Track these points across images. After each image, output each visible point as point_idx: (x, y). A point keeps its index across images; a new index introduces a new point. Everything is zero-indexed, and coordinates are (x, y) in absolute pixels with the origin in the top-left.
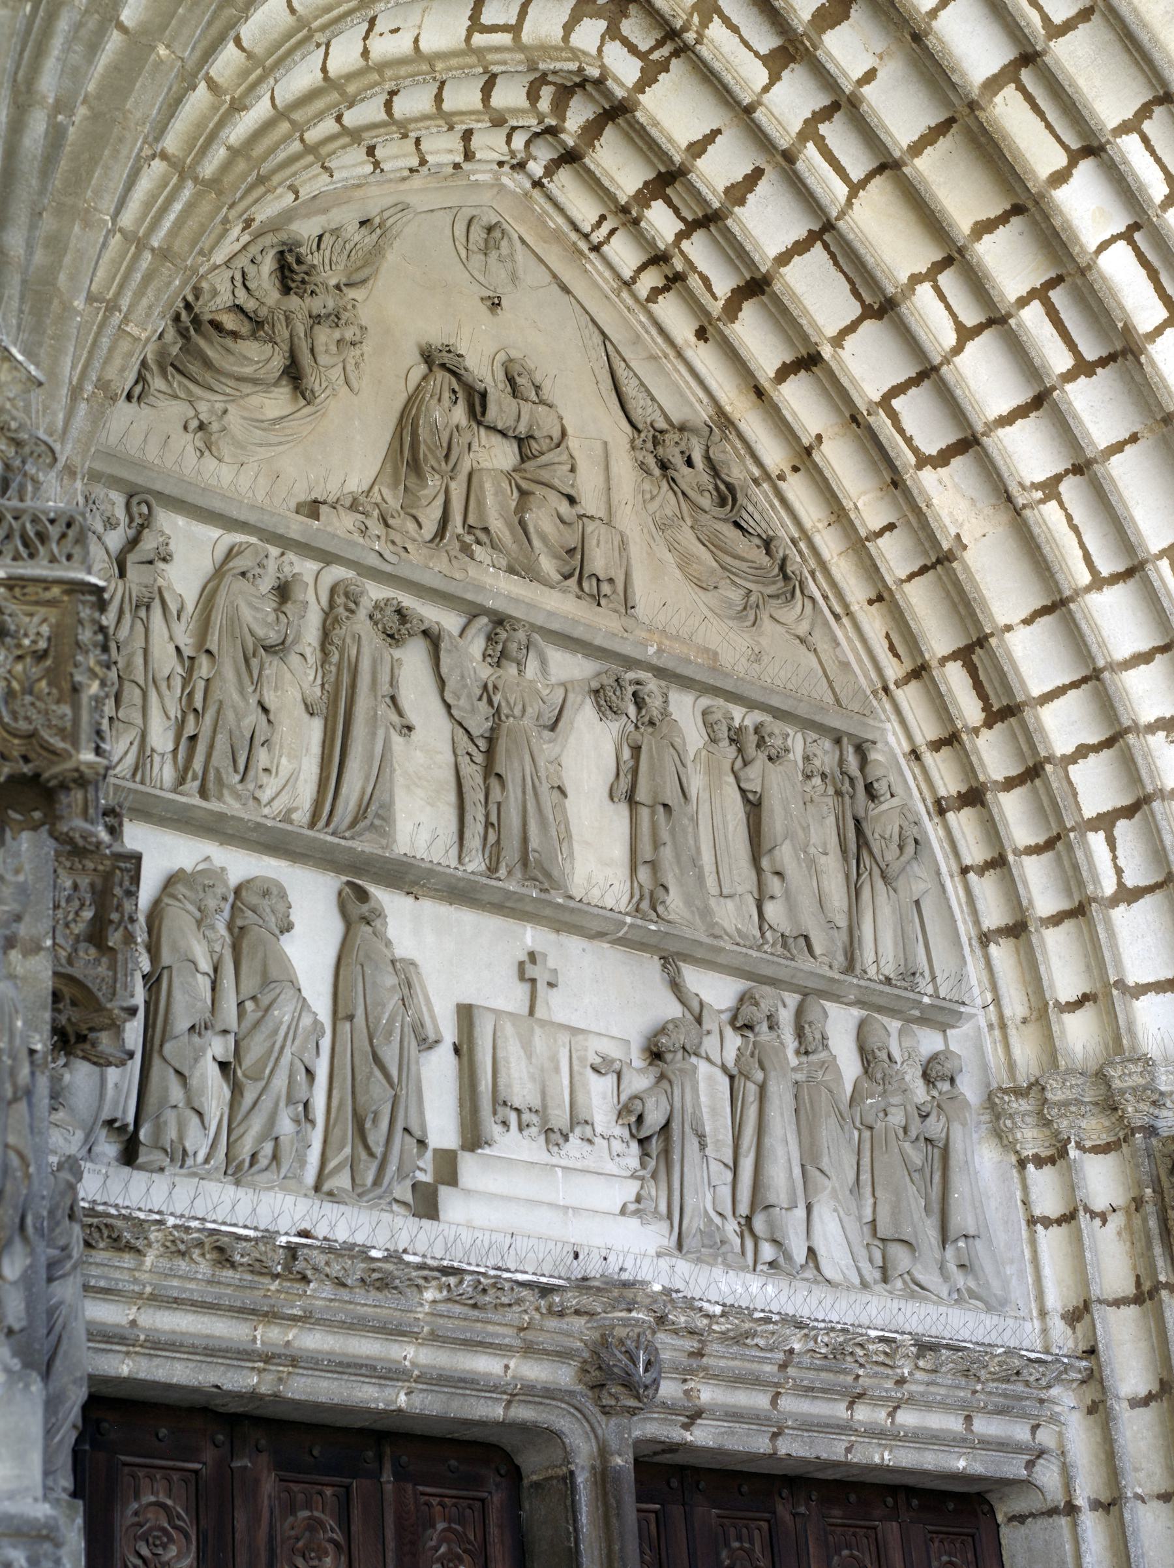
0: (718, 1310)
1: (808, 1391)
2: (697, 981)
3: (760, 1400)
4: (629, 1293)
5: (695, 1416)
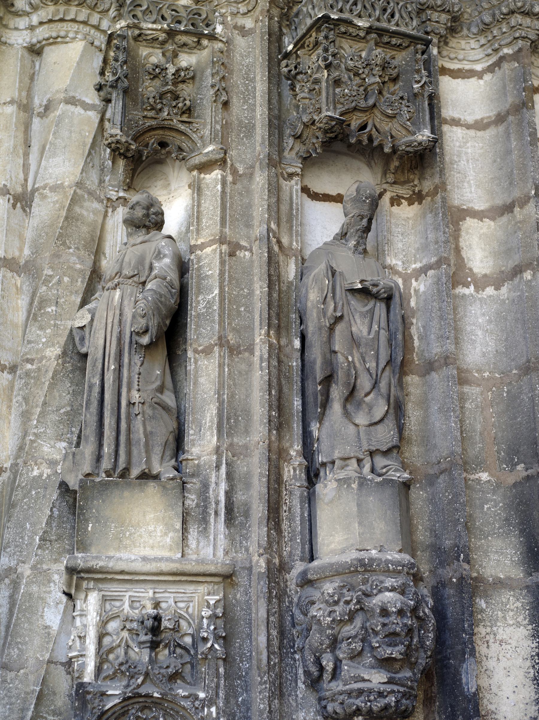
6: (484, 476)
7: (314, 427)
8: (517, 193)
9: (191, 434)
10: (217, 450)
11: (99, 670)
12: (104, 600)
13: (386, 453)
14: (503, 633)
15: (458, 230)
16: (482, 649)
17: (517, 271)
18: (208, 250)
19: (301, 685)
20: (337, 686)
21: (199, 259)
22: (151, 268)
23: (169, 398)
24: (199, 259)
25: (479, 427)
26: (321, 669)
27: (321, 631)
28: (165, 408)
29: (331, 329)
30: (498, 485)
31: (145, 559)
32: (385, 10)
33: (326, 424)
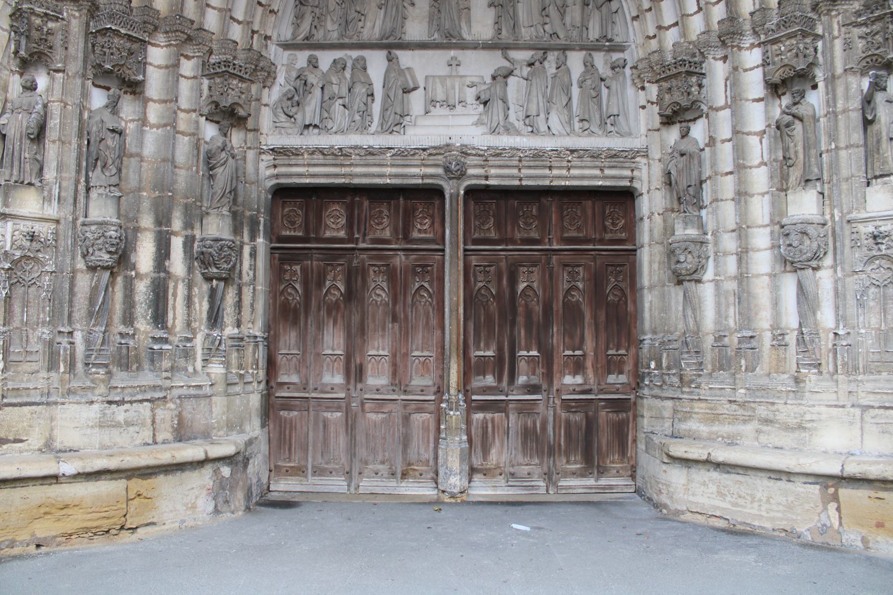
0: (486, 148)
1: (530, 167)
2: (513, 54)
3: (515, 171)
4: (449, 148)
5: (487, 178)
6: (145, 194)
7: (90, 174)
8: (169, 98)
9: (46, 170)
10: (56, 178)
11: (11, 247)
12: (14, 224)
13: (114, 186)
14: (145, 244)
15: (146, 106)
16: (138, 249)
17: (165, 125)
18: (56, 104)
19: (79, 256)
20: (93, 258)
21: (52, 106)
22: (34, 108)
23: (38, 157)
24: (52, 106)
25: (145, 177)
26: (88, 252)
27: (90, 241)
28: (37, 160)
29: (100, 142)
30: (149, 197)
31: (30, 213)
32: (131, 26)
33: (95, 172)
